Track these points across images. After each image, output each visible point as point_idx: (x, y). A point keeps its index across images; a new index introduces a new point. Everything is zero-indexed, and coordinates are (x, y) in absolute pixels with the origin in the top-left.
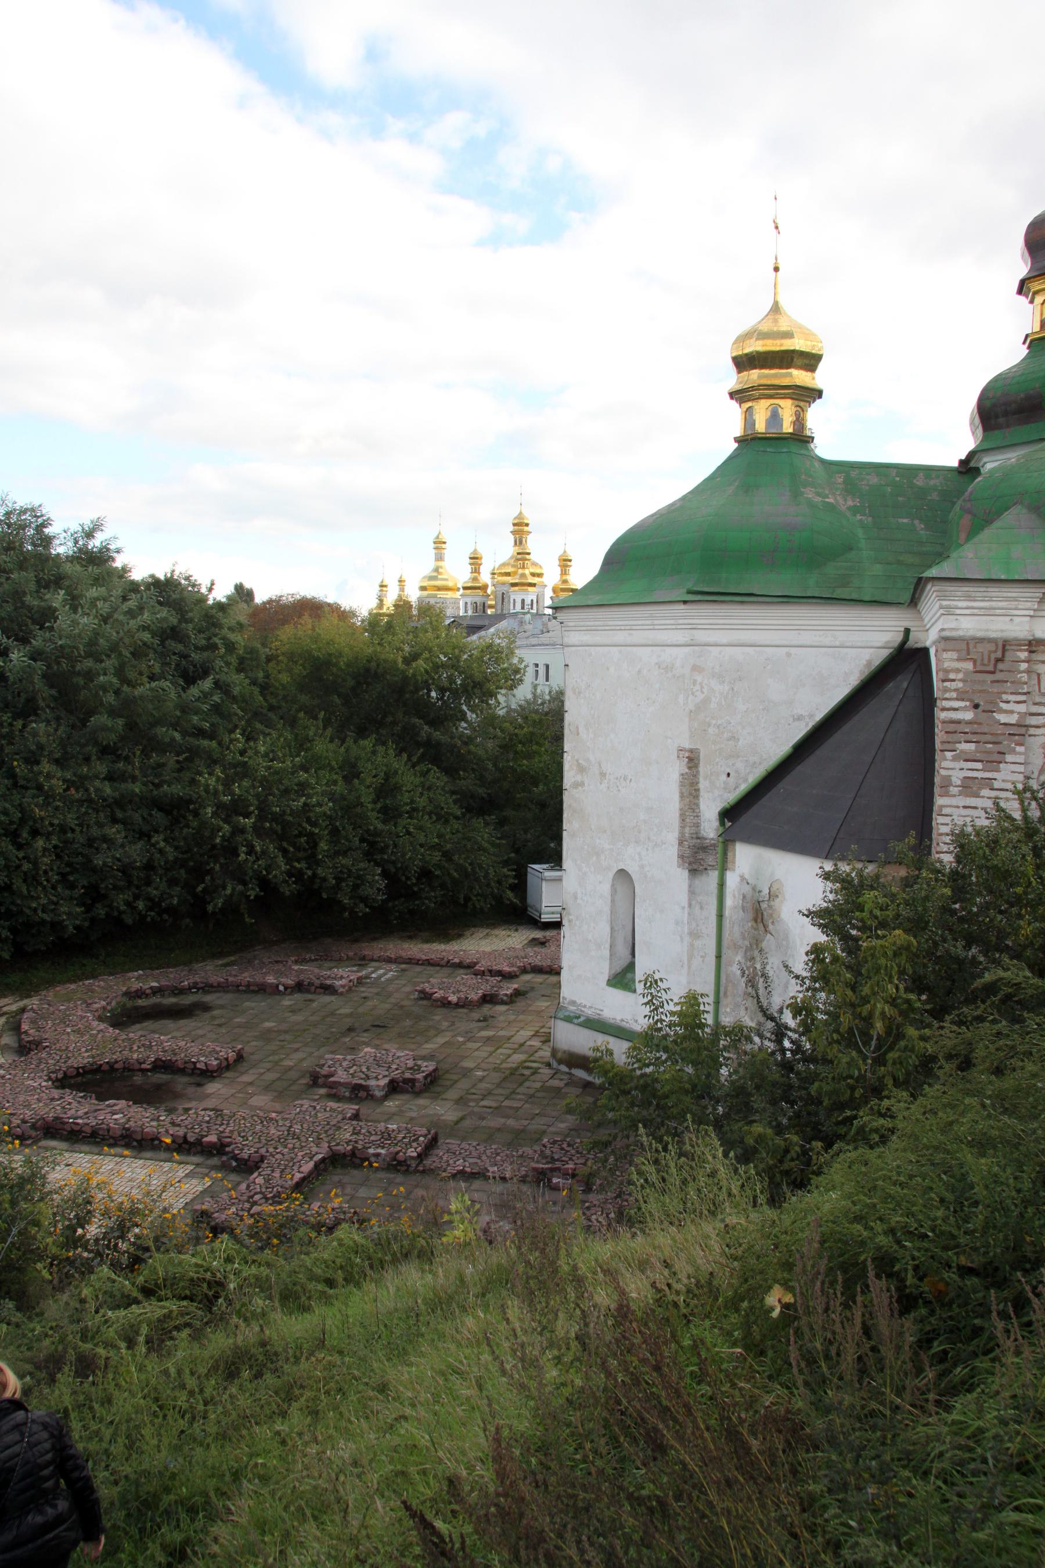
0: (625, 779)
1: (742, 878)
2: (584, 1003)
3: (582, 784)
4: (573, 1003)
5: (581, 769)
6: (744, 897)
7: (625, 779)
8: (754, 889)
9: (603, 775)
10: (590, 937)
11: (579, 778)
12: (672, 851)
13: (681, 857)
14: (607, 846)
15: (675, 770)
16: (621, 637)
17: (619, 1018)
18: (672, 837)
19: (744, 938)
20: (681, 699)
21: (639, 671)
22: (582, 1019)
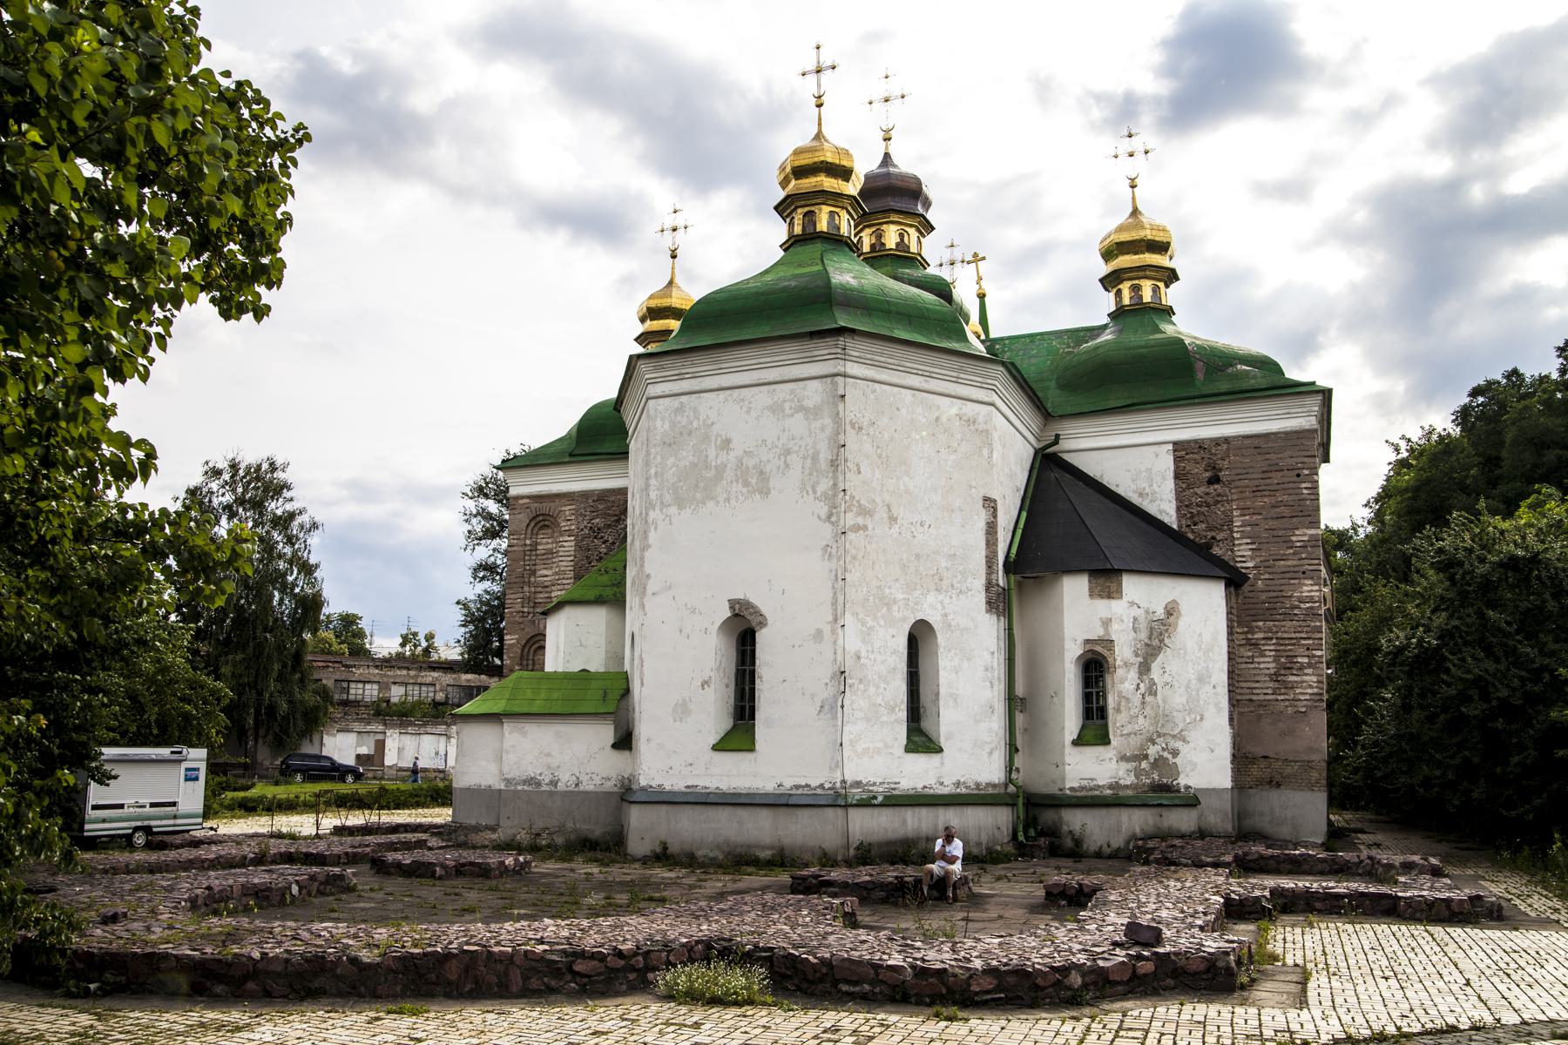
0: (922, 525)
1: (1132, 603)
2: (873, 780)
3: (865, 528)
4: (858, 784)
5: (865, 512)
6: (1135, 619)
7: (922, 525)
8: (1147, 612)
9: (893, 519)
10: (879, 700)
11: (860, 520)
12: (981, 598)
13: (989, 603)
14: (900, 596)
15: (980, 519)
16: (915, 381)
17: (919, 786)
18: (979, 583)
19: (1137, 655)
20: (985, 452)
21: (937, 419)
22: (880, 799)
